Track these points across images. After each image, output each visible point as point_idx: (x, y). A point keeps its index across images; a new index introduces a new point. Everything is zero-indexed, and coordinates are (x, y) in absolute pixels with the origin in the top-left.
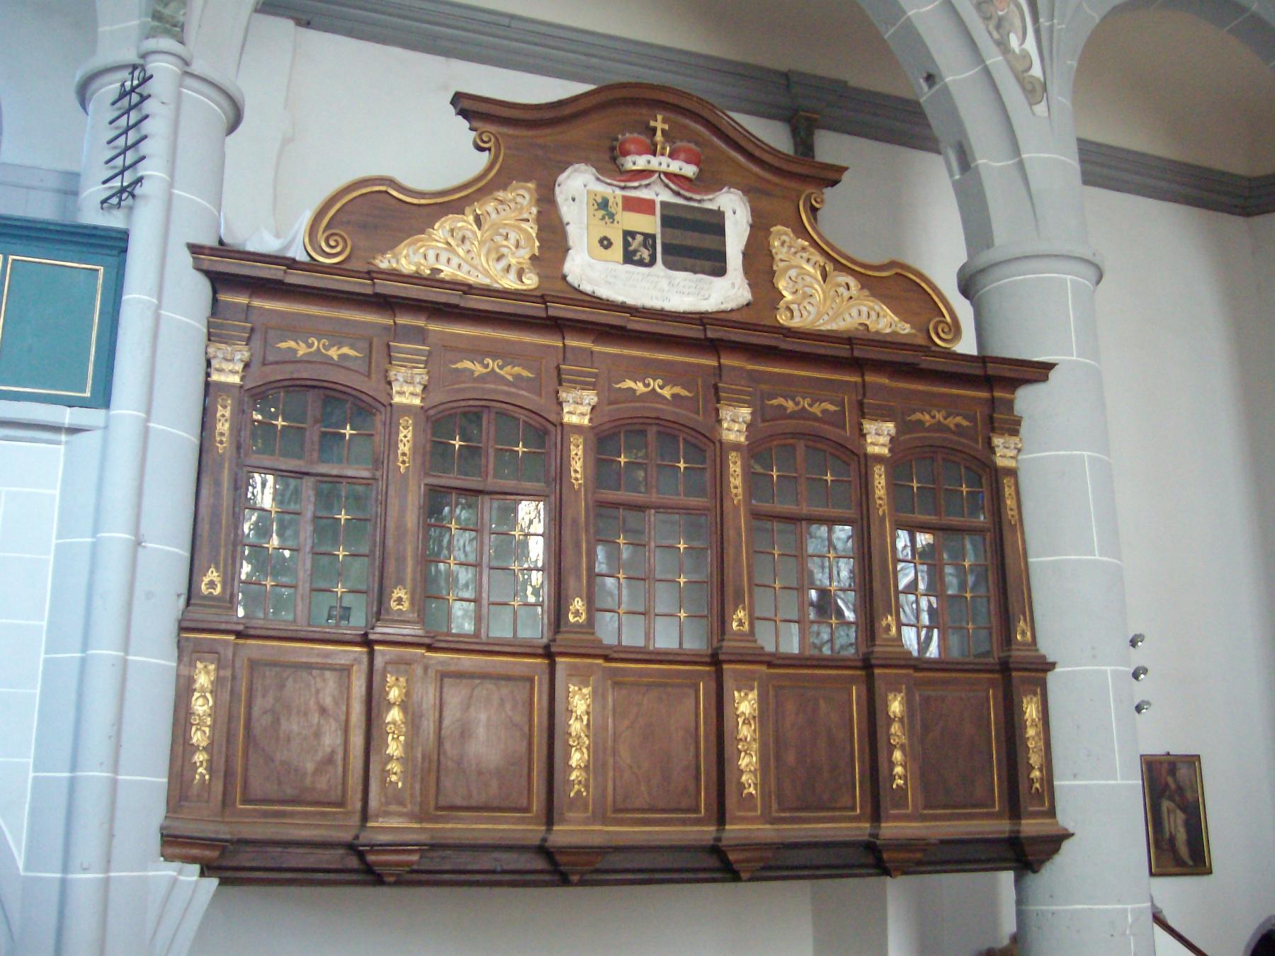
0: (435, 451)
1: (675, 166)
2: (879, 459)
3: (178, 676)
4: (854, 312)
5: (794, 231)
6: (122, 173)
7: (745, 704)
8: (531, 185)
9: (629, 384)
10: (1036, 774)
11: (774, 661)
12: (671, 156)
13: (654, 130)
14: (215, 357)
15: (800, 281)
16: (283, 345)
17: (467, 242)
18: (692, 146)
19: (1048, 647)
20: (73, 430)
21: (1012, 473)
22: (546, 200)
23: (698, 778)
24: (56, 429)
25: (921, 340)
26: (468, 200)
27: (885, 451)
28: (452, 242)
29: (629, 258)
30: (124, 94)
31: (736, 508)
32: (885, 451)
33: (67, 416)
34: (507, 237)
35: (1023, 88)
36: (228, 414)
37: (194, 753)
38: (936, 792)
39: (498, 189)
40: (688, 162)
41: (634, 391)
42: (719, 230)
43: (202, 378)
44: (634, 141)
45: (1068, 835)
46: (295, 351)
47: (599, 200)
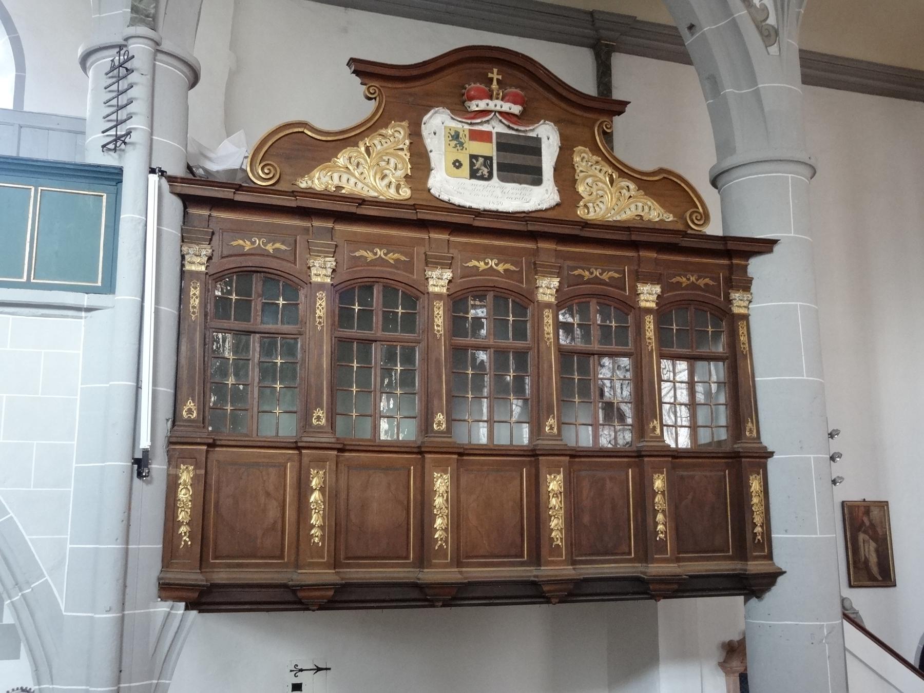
0: (342, 317)
1: (506, 107)
2: (648, 311)
3: (168, 475)
4: (633, 207)
5: (591, 150)
6: (116, 126)
7: (554, 484)
10: (758, 529)
11: (575, 454)
12: (502, 100)
13: (491, 80)
14: (188, 253)
15: (594, 186)
16: (234, 243)
17: (361, 167)
18: (518, 91)
19: (768, 440)
20: (89, 310)
21: (745, 317)
22: (415, 134)
23: (522, 535)
24: (79, 309)
25: (680, 227)
26: (361, 136)
27: (653, 305)
28: (350, 167)
29: (474, 174)
30: (113, 68)
32: (653, 305)
33: (85, 300)
34: (388, 163)
35: (761, 33)
36: (198, 293)
37: (180, 527)
38: (686, 542)
40: (515, 103)
41: (478, 268)
44: (478, 89)
45: (782, 573)
47: (453, 134)
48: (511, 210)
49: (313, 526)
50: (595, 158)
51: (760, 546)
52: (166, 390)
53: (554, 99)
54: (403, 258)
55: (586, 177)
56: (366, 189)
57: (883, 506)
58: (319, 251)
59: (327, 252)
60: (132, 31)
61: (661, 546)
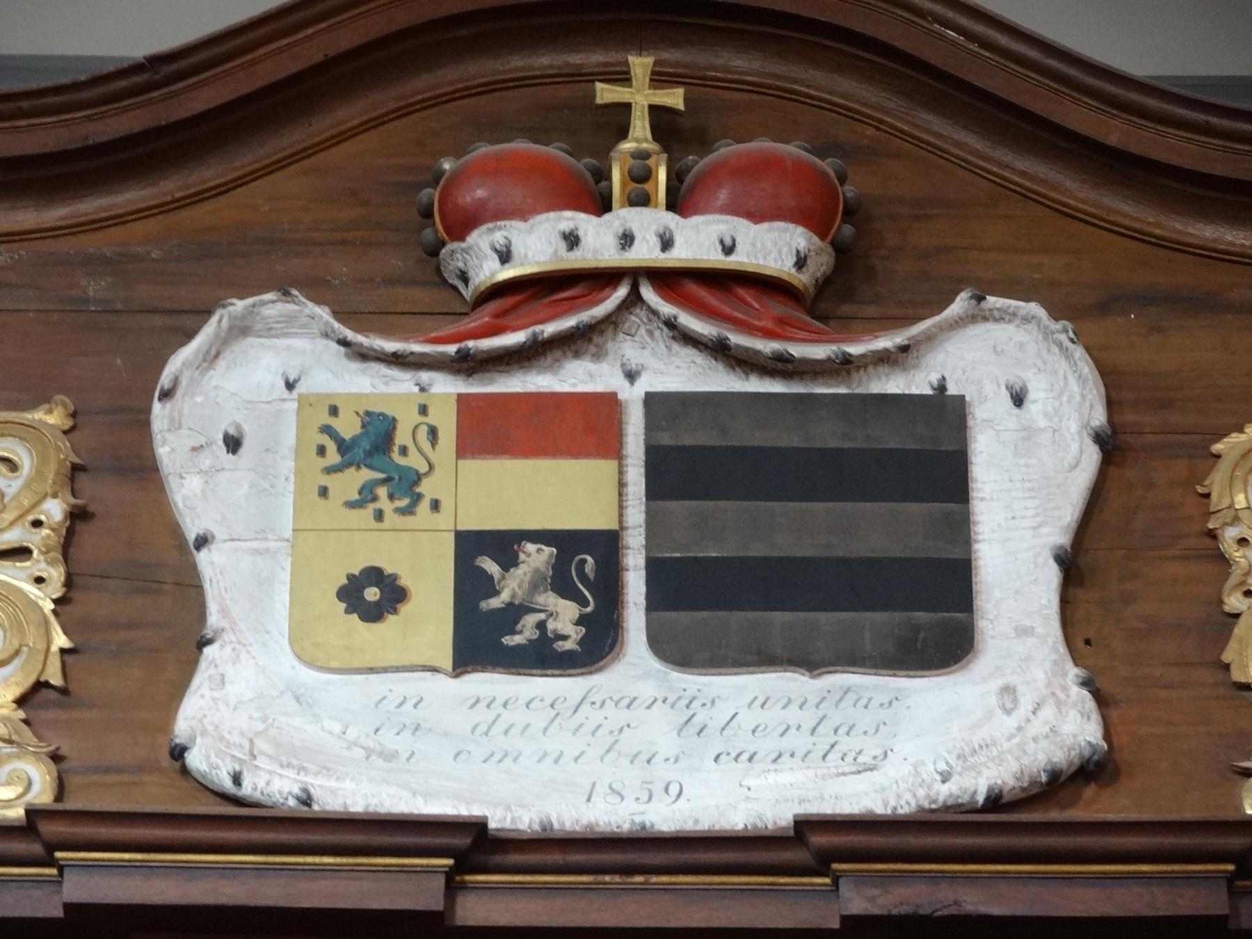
12: (677, 203)
18: (791, 150)
29: (482, 642)
47: (349, 427)
53: (1075, 189)
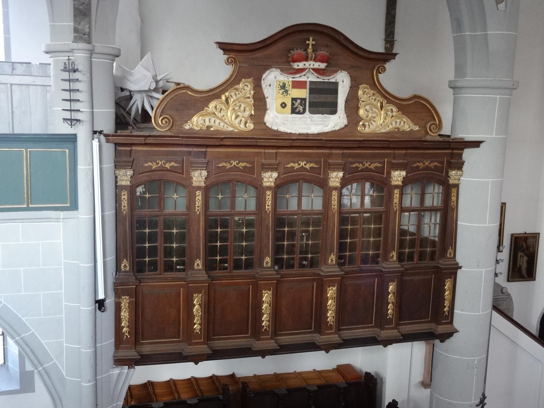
4: (394, 123)
8: (250, 80)
9: (292, 164)
10: (446, 309)
13: (309, 44)
16: (146, 165)
19: (460, 259)
21: (457, 186)
23: (311, 318)
26: (223, 91)
28: (216, 113)
29: (294, 111)
31: (334, 214)
39: (236, 85)
40: (322, 62)
42: (335, 91)
43: (114, 185)
45: (457, 331)
46: (152, 167)
47: (281, 84)
48: (316, 132)
49: (195, 324)
50: (372, 92)
51: (447, 317)
52: (111, 258)
54: (248, 165)
55: (365, 105)
56: (226, 126)
57: (536, 237)
58: (197, 167)
59: (202, 167)
60: (75, 45)
61: (390, 321)
